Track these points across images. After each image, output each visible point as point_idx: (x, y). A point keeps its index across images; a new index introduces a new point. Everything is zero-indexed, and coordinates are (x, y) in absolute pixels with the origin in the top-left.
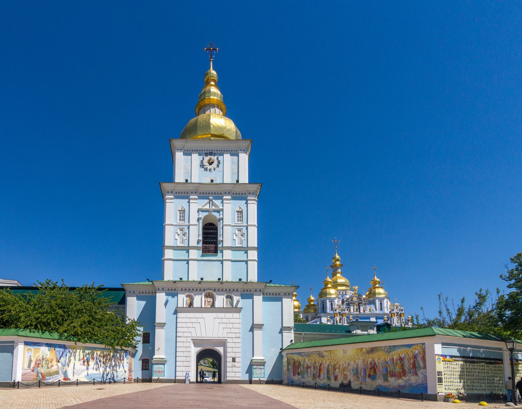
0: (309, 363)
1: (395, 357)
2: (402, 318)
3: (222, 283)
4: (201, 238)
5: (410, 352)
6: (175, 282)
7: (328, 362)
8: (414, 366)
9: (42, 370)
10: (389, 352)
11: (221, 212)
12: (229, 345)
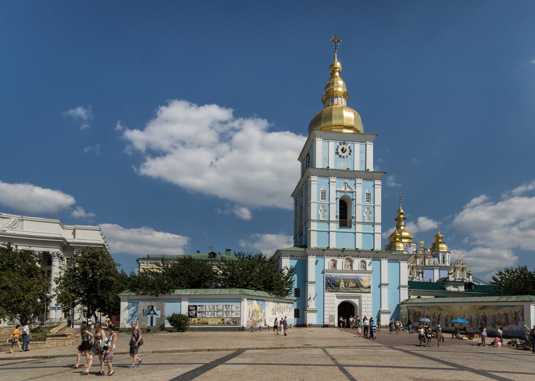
0: (429, 314)
1: (501, 313)
2: (465, 272)
3: (359, 251)
4: (338, 215)
5: (513, 310)
6: (324, 250)
7: (446, 314)
8: (515, 319)
9: (255, 318)
10: (497, 309)
12: (363, 299)
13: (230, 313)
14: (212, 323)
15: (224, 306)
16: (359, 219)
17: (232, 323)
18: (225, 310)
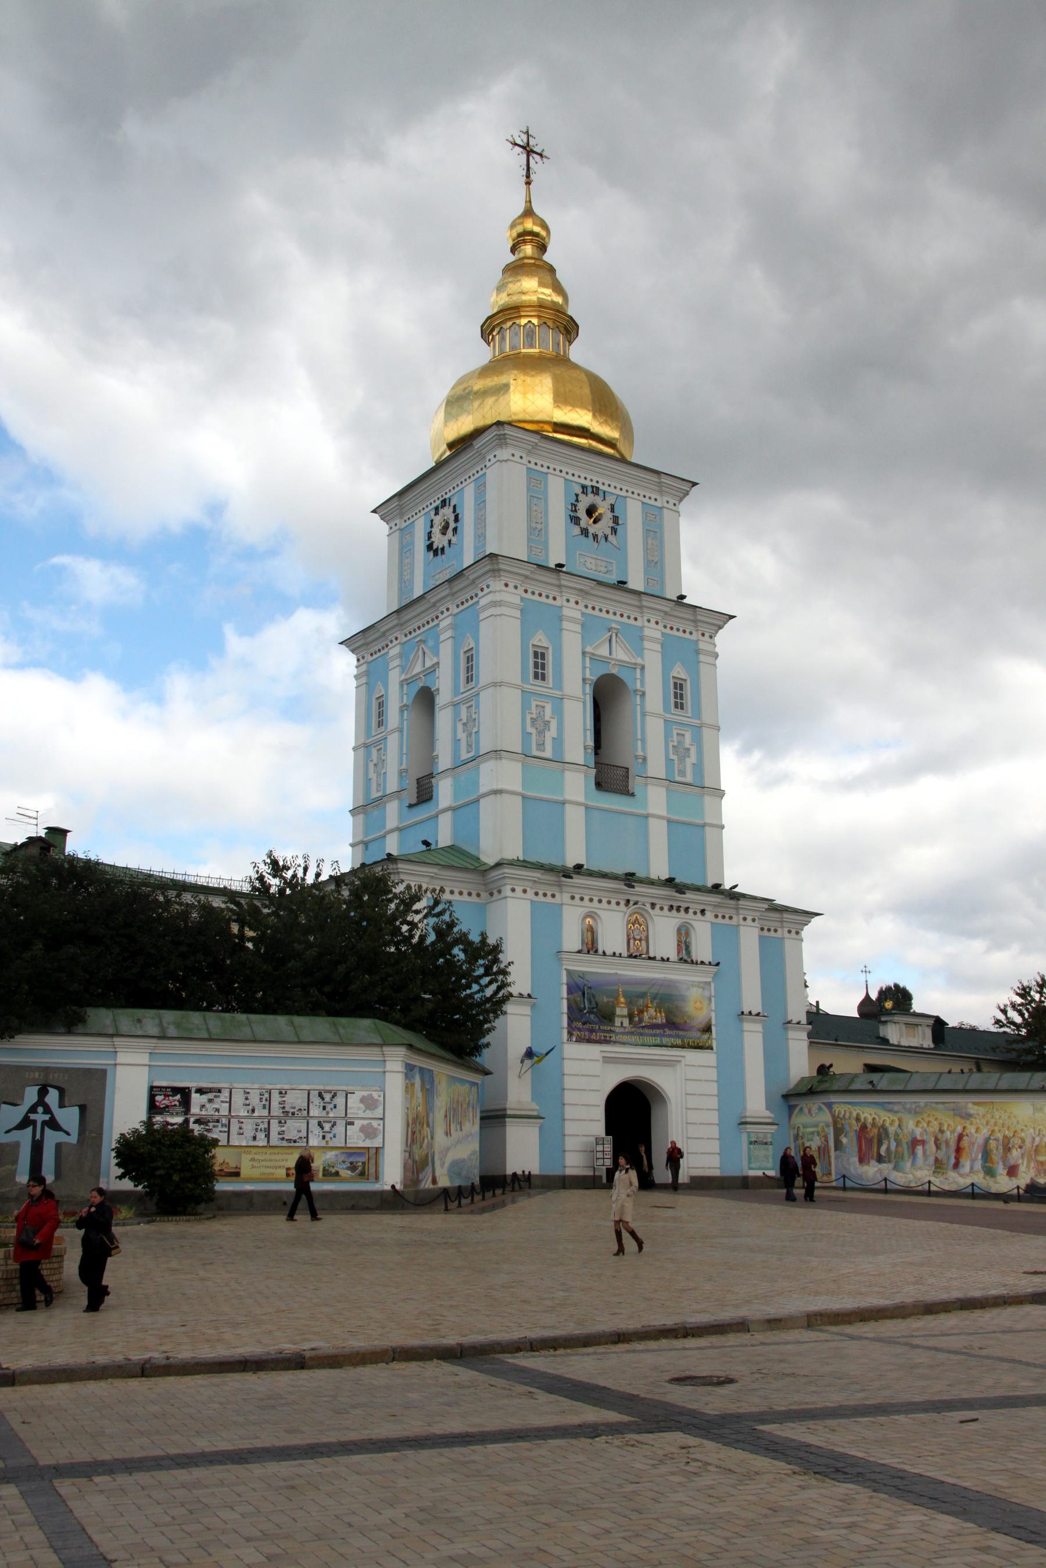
11: (638, 671)
13: (340, 1129)
14: (256, 1173)
15: (315, 1099)
16: (656, 766)
17: (345, 1173)
18: (315, 1112)
